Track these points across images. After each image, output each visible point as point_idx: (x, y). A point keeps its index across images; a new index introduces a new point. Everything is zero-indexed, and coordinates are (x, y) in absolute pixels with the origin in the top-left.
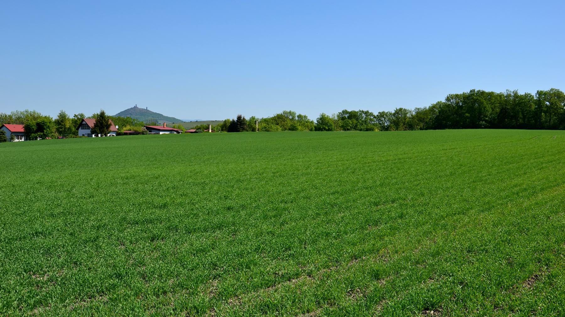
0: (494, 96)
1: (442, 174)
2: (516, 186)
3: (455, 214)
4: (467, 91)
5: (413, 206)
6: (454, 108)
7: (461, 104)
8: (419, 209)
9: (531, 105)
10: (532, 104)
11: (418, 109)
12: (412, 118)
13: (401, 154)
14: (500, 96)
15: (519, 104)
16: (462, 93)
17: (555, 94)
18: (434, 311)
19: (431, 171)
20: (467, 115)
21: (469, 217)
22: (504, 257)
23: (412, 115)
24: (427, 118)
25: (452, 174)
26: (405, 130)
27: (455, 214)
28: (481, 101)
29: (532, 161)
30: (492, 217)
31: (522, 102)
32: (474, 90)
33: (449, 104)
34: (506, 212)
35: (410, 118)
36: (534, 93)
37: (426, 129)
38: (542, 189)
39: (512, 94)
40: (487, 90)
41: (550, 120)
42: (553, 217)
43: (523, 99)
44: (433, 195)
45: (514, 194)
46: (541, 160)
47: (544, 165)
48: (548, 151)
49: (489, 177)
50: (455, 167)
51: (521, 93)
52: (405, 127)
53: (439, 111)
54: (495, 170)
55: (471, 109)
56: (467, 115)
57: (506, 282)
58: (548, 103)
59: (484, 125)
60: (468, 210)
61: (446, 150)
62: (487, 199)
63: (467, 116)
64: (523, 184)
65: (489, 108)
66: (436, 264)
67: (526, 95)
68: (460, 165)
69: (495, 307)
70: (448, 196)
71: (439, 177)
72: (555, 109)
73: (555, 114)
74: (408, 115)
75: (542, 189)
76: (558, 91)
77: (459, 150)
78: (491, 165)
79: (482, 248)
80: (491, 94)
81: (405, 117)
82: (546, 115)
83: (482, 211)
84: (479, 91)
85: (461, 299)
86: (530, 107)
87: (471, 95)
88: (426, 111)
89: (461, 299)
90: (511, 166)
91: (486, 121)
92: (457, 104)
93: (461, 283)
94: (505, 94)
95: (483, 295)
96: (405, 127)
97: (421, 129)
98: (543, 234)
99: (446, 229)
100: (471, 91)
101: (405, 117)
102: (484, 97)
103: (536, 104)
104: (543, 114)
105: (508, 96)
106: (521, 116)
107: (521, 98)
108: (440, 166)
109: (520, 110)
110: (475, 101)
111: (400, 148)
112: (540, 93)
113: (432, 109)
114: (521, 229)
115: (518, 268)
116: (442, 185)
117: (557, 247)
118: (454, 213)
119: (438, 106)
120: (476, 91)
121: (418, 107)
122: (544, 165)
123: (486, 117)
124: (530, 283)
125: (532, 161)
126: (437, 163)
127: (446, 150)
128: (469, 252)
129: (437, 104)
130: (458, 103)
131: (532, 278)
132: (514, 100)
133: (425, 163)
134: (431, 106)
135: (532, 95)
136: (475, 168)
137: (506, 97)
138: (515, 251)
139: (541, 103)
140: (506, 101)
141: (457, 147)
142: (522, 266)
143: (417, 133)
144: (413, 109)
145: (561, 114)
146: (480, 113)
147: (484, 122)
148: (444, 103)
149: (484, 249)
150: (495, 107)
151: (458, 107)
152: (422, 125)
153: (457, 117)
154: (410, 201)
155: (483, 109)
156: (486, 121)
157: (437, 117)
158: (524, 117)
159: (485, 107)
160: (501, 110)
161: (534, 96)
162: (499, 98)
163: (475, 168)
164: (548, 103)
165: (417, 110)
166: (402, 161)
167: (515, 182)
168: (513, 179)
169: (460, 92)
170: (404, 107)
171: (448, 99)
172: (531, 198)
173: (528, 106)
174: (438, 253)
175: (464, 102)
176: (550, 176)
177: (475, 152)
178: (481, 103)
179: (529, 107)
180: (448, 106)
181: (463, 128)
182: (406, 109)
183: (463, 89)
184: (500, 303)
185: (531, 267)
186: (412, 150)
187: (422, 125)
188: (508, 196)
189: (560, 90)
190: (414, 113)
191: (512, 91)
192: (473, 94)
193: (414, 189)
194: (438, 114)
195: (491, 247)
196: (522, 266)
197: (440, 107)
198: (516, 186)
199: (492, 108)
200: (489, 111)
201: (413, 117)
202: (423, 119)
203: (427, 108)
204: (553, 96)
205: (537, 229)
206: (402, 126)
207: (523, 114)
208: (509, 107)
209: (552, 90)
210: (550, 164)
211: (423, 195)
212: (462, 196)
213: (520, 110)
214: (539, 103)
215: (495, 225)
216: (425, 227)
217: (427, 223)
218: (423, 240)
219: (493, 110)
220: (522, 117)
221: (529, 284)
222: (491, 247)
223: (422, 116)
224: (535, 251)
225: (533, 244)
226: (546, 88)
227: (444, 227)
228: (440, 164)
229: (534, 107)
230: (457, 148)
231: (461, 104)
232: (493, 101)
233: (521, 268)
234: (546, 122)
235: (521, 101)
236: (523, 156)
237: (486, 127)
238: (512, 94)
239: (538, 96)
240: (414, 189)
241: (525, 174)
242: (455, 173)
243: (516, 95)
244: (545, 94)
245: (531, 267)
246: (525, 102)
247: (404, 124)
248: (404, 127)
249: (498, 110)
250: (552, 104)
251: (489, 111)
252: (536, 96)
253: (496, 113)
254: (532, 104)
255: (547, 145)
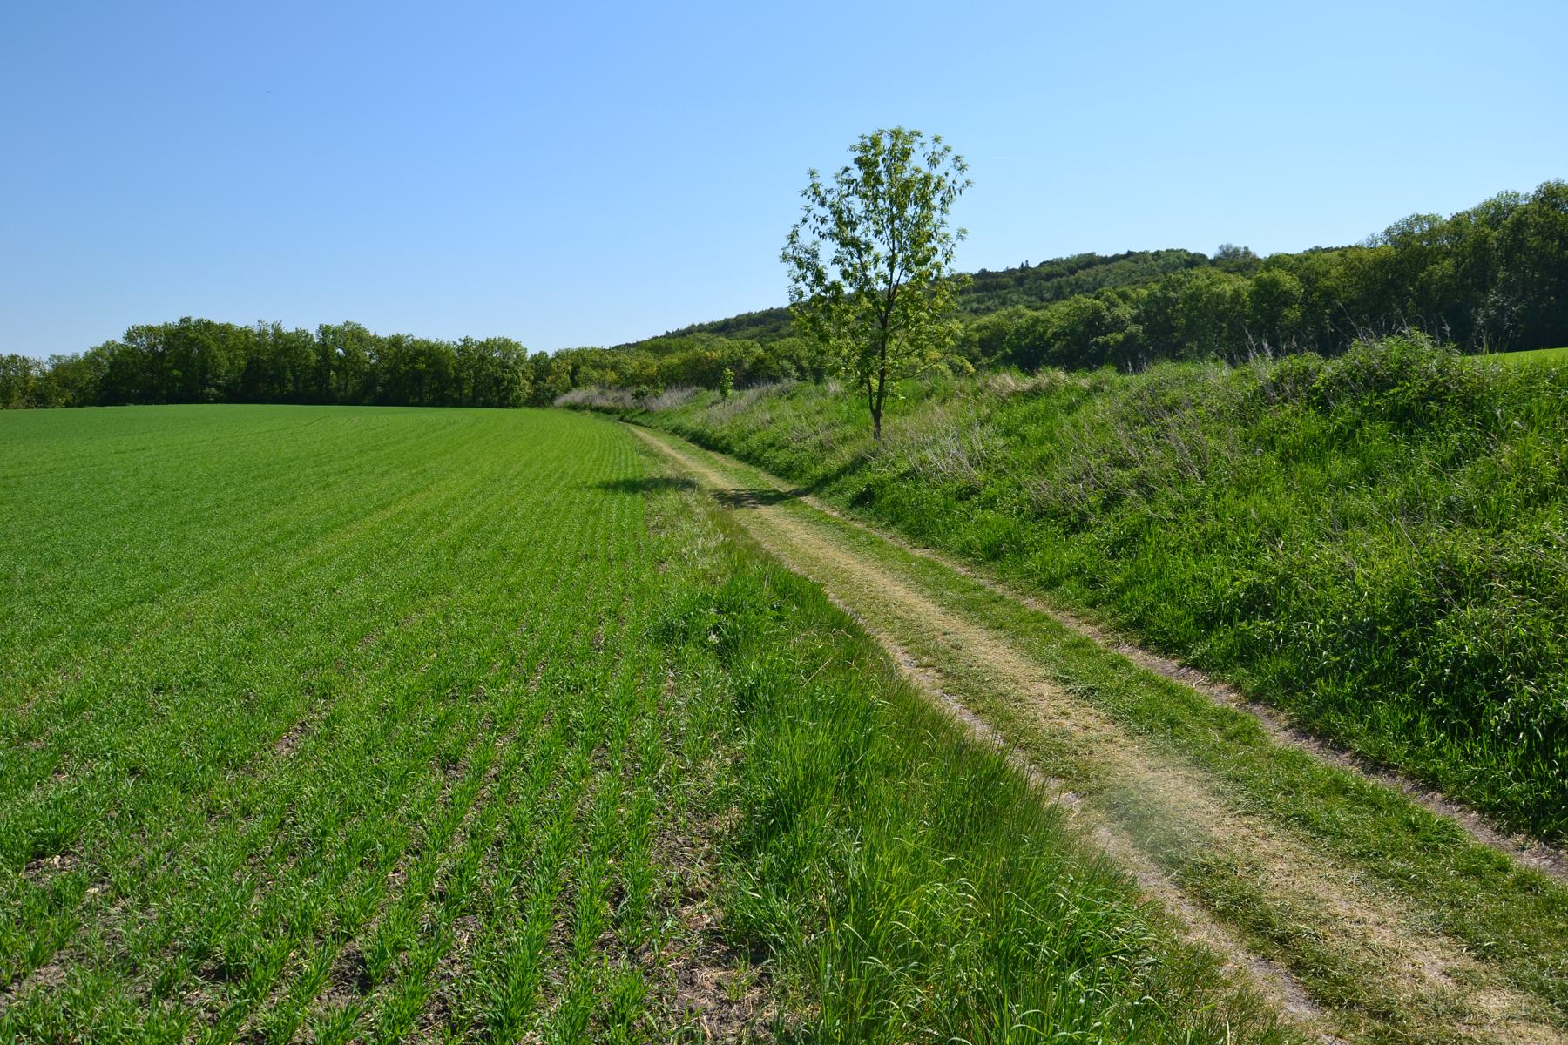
0: (232, 334)
1: (109, 509)
2: (271, 527)
3: (132, 603)
4: (173, 319)
5: (30, 592)
6: (145, 357)
7: (160, 349)
8: (45, 598)
9: (308, 354)
10: (311, 351)
11: (59, 358)
12: (45, 380)
13: (11, 467)
14: (246, 333)
15: (286, 351)
16: (161, 324)
17: (352, 331)
18: (62, 857)
19: (83, 503)
20: (175, 372)
21: (165, 607)
22: (235, 693)
23: (44, 373)
24: (83, 379)
25: (133, 508)
26: (28, 407)
27: (132, 603)
28: (206, 342)
29: (309, 471)
30: (217, 600)
31: (290, 348)
32: (189, 319)
33: (133, 349)
34: (247, 586)
35: (38, 379)
36: (313, 330)
37: (81, 405)
38: (325, 531)
39: (271, 331)
40: (218, 319)
41: (346, 385)
42: (342, 589)
43: (292, 342)
44: (82, 561)
45: (267, 544)
46: (326, 468)
47: (331, 479)
48: (340, 450)
49: (217, 510)
50: (143, 491)
51: (288, 328)
52: (28, 401)
53: (110, 363)
54: (232, 494)
55: (184, 361)
56: (175, 372)
57: (238, 749)
58: (340, 351)
59: (213, 395)
60: (162, 590)
61: (125, 452)
62: (210, 560)
63: (176, 377)
64: (286, 521)
65: (222, 357)
66: (74, 735)
67: (300, 334)
68: (154, 486)
69: (211, 813)
70: (119, 561)
71: (103, 516)
72: (355, 364)
73: (356, 373)
74: (32, 372)
75: (325, 531)
76: (359, 328)
77: (154, 451)
78: (223, 484)
79: (188, 678)
80: (225, 330)
81: (25, 376)
82: (338, 375)
83: (196, 590)
84: (200, 321)
85: (131, 812)
86: (307, 358)
87: (183, 329)
88: (79, 362)
89: (131, 812)
90: (265, 483)
91: (218, 387)
92: (152, 347)
93: (133, 772)
94: (256, 330)
95: (184, 792)
96: (28, 401)
97: (68, 405)
98: (320, 628)
99: (105, 643)
100: (182, 320)
101: (25, 376)
102: (211, 334)
103: (316, 350)
104: (332, 373)
105: (262, 334)
106: (289, 375)
107: (288, 338)
108: (106, 490)
109: (287, 364)
110: (193, 342)
111: (11, 450)
112: (325, 330)
113: (93, 358)
114: (277, 623)
115: (265, 714)
116: (108, 537)
117: (345, 653)
118: (129, 600)
119: (107, 353)
120: (193, 320)
121: (57, 354)
122: (331, 479)
123: (219, 377)
124: (291, 743)
125: (309, 471)
126: (100, 484)
127: (125, 452)
128: (158, 690)
129: (104, 348)
130: (155, 346)
131: (296, 730)
132: (276, 343)
133: (71, 484)
134: (90, 351)
135: (310, 332)
136: (188, 491)
137: (258, 335)
138: (261, 675)
139: (327, 351)
140: (257, 344)
141: (151, 445)
142: (274, 708)
143: (57, 416)
144: (45, 358)
145: (366, 373)
146: (204, 370)
147: (213, 390)
148: (121, 345)
149: (193, 679)
150: (236, 356)
151: (154, 354)
152: (69, 395)
153: (153, 378)
154: (22, 580)
155: (209, 360)
156: (218, 387)
157: (107, 376)
158: (297, 379)
159: (215, 357)
160: (249, 363)
161: (315, 336)
162: (243, 338)
163: (188, 491)
164: (340, 351)
165: (56, 361)
166: (12, 482)
167: (270, 518)
168: (269, 511)
169: (157, 322)
170: (21, 352)
171: (130, 336)
172: (301, 552)
173: (304, 355)
174: (81, 706)
175: (168, 345)
176: (341, 502)
177: (189, 455)
178: (205, 348)
179: (306, 358)
180: (132, 352)
181: (167, 403)
182: (26, 356)
183: (165, 313)
184: (223, 802)
185: (293, 706)
186: (39, 456)
187: (69, 395)
188: (253, 551)
189: (362, 326)
190: (48, 368)
191: (270, 323)
192: (188, 328)
193: (34, 552)
194: (108, 371)
195: (207, 672)
196: (274, 708)
197: (112, 354)
198: (271, 527)
199: (229, 359)
200: (225, 366)
201: (47, 378)
202: (73, 382)
203: (81, 356)
204: (350, 336)
205: (308, 621)
206: (19, 398)
207: (293, 372)
208: (265, 358)
209: (347, 324)
210: (343, 476)
211: (57, 563)
212: (152, 558)
213: (287, 364)
214: (323, 349)
215: (223, 621)
216: (54, 646)
217: (60, 632)
218: (45, 677)
219: (232, 363)
220: (292, 378)
221: (288, 744)
222: (207, 672)
223: (68, 374)
224: (301, 670)
225: (299, 654)
226: (336, 321)
227: (103, 637)
228: (107, 487)
229: (314, 358)
230: (151, 449)
231: (160, 349)
232: (231, 343)
233: (270, 712)
234: (339, 389)
235: (289, 345)
236: (291, 460)
237: (218, 401)
238: (271, 331)
239: (321, 335)
240: (34, 552)
241: (293, 499)
242: (141, 506)
243: (278, 333)
244: (335, 332)
245: (293, 706)
246: (295, 348)
247: (24, 394)
248: (24, 401)
249: (243, 363)
250: (347, 352)
251: (225, 366)
252: (317, 335)
253: (240, 370)
254: (311, 351)
255: (338, 437)
